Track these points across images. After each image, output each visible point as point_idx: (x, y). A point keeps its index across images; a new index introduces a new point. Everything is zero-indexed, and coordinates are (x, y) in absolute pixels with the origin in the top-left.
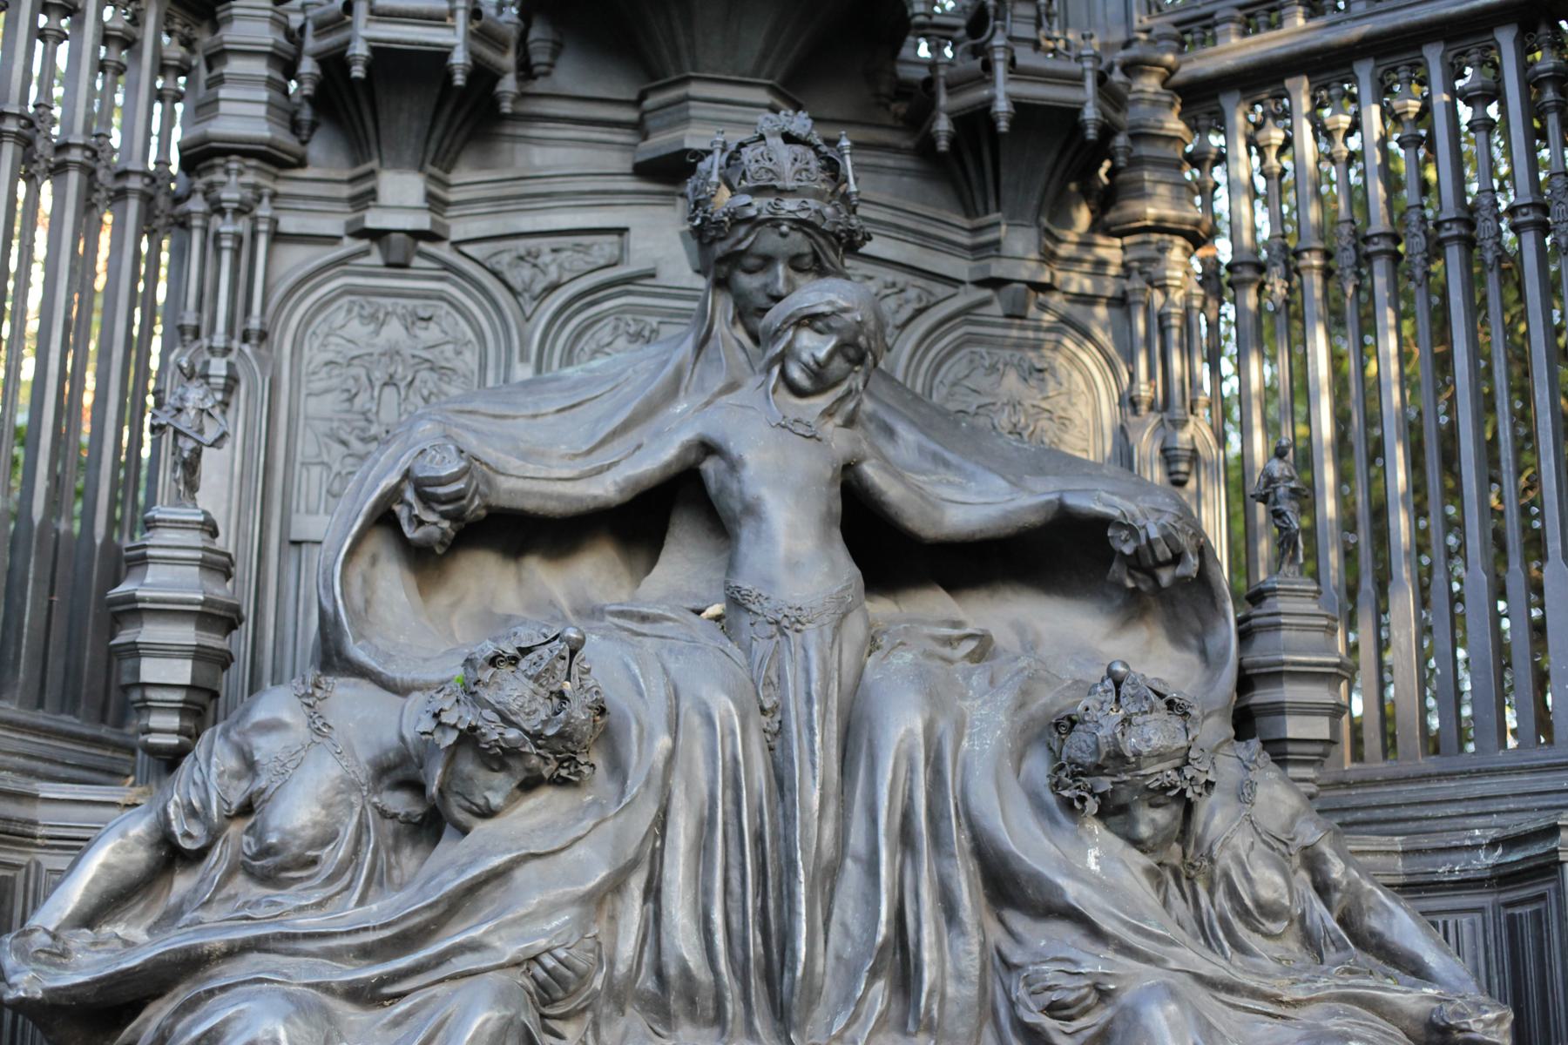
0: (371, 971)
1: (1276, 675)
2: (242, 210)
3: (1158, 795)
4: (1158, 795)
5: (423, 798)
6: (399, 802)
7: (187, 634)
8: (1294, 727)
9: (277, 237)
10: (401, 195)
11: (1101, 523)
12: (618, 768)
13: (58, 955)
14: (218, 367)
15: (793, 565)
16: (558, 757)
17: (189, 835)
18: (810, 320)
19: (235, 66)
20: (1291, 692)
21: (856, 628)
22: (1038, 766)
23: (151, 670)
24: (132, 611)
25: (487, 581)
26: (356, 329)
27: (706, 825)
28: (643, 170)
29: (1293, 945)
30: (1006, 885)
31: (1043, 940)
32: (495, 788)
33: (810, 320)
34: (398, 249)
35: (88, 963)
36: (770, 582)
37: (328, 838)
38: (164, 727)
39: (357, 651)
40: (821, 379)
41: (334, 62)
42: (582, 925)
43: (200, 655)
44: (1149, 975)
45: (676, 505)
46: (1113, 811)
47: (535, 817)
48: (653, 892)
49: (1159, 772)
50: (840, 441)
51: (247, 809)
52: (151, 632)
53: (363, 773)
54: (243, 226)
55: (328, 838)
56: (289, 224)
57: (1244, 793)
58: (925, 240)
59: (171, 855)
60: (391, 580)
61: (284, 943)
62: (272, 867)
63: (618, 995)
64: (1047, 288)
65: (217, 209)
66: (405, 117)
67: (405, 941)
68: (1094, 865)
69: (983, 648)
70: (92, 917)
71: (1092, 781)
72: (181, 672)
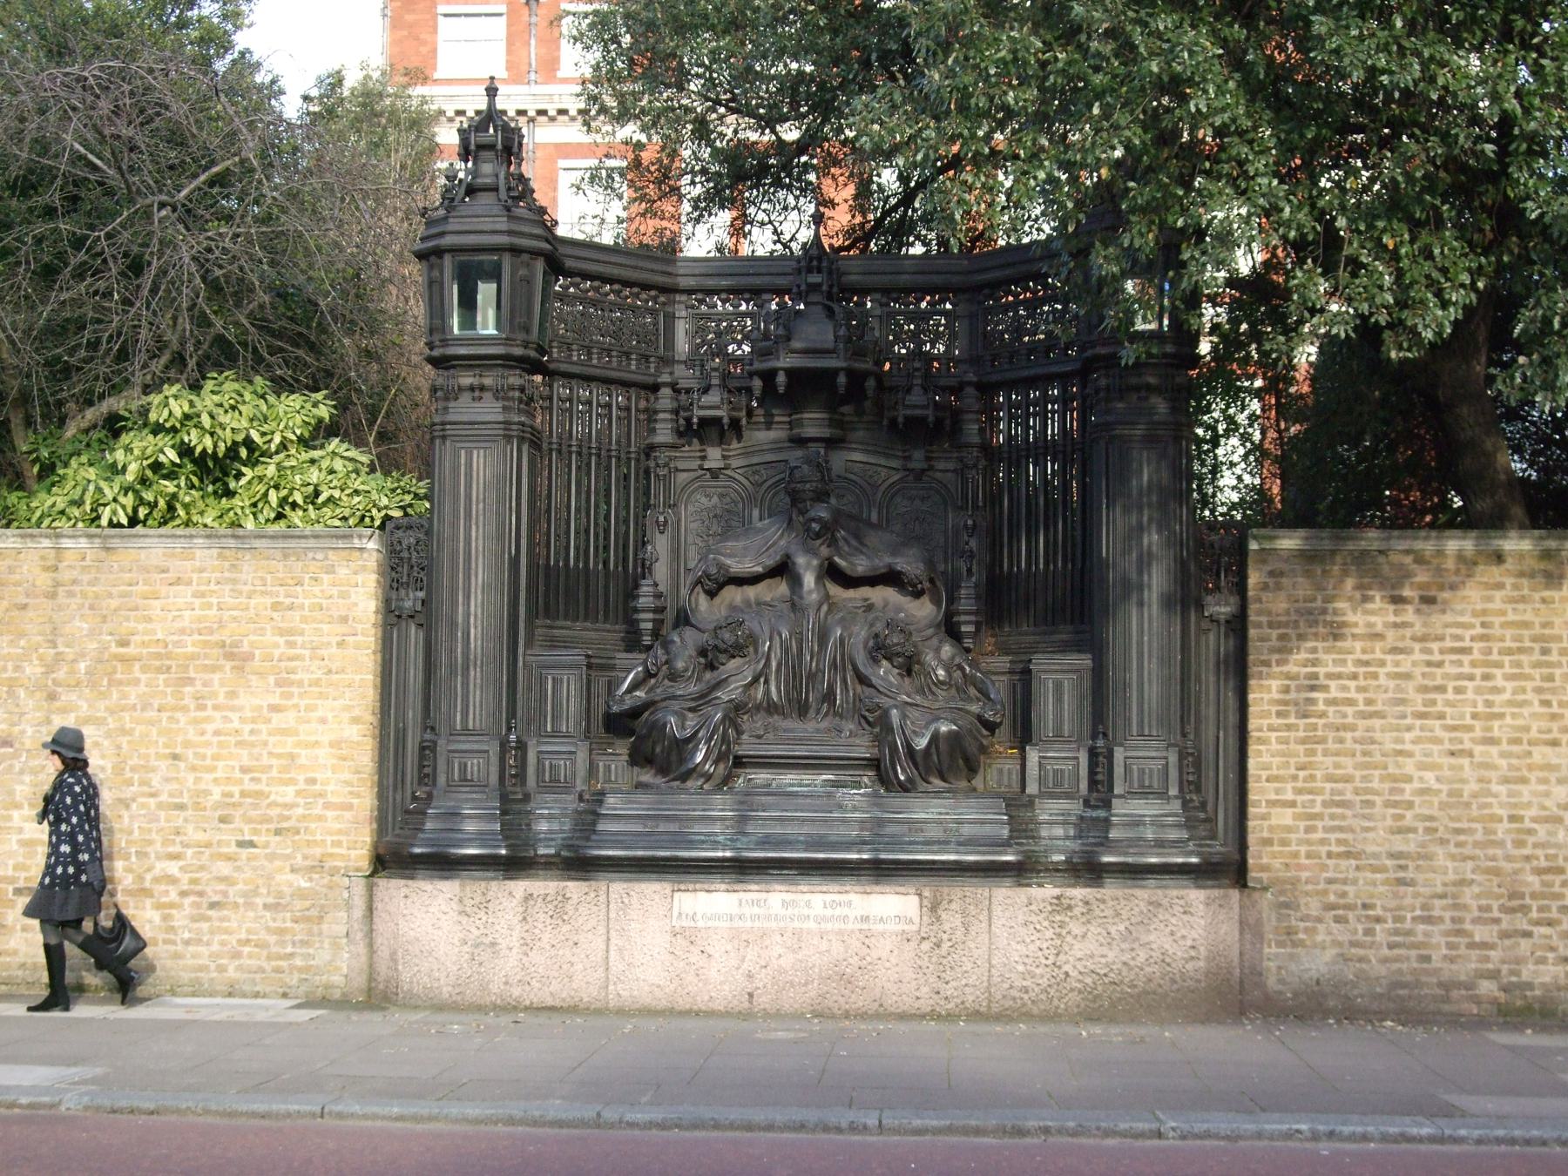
0: (693, 704)
1: (959, 614)
2: (666, 465)
3: (898, 655)
4: (898, 655)
5: (710, 657)
6: (702, 660)
7: (650, 616)
8: (963, 629)
9: (677, 470)
10: (714, 456)
11: (900, 573)
12: (756, 651)
13: (622, 700)
14: (661, 519)
15: (810, 592)
16: (736, 650)
17: (653, 670)
18: (813, 520)
19: (661, 416)
20: (963, 618)
21: (825, 608)
22: (871, 643)
23: (643, 625)
24: (636, 610)
25: (732, 594)
26: (704, 500)
27: (779, 665)
28: (791, 440)
29: (953, 691)
30: (863, 680)
31: (868, 691)
32: (723, 658)
33: (813, 520)
34: (715, 474)
35: (628, 703)
36: (801, 598)
37: (686, 670)
38: (647, 640)
39: (693, 621)
40: (818, 536)
41: (688, 420)
42: (744, 692)
43: (654, 621)
44: (891, 702)
45: (783, 570)
46: (888, 659)
47: (733, 664)
48: (766, 682)
49: (899, 649)
50: (825, 551)
51: (666, 662)
52: (642, 616)
53: (694, 654)
54: (666, 471)
55: (686, 670)
56: (681, 465)
57: (938, 650)
58: (887, 456)
59: (649, 675)
60: (703, 600)
61: (674, 698)
62: (673, 676)
63: (758, 708)
64: (931, 468)
65: (658, 465)
66: (713, 433)
67: (702, 696)
68: (884, 673)
69: (870, 608)
70: (630, 690)
71: (879, 650)
72: (650, 625)
